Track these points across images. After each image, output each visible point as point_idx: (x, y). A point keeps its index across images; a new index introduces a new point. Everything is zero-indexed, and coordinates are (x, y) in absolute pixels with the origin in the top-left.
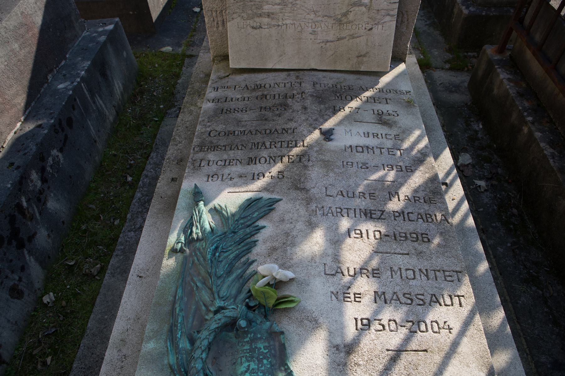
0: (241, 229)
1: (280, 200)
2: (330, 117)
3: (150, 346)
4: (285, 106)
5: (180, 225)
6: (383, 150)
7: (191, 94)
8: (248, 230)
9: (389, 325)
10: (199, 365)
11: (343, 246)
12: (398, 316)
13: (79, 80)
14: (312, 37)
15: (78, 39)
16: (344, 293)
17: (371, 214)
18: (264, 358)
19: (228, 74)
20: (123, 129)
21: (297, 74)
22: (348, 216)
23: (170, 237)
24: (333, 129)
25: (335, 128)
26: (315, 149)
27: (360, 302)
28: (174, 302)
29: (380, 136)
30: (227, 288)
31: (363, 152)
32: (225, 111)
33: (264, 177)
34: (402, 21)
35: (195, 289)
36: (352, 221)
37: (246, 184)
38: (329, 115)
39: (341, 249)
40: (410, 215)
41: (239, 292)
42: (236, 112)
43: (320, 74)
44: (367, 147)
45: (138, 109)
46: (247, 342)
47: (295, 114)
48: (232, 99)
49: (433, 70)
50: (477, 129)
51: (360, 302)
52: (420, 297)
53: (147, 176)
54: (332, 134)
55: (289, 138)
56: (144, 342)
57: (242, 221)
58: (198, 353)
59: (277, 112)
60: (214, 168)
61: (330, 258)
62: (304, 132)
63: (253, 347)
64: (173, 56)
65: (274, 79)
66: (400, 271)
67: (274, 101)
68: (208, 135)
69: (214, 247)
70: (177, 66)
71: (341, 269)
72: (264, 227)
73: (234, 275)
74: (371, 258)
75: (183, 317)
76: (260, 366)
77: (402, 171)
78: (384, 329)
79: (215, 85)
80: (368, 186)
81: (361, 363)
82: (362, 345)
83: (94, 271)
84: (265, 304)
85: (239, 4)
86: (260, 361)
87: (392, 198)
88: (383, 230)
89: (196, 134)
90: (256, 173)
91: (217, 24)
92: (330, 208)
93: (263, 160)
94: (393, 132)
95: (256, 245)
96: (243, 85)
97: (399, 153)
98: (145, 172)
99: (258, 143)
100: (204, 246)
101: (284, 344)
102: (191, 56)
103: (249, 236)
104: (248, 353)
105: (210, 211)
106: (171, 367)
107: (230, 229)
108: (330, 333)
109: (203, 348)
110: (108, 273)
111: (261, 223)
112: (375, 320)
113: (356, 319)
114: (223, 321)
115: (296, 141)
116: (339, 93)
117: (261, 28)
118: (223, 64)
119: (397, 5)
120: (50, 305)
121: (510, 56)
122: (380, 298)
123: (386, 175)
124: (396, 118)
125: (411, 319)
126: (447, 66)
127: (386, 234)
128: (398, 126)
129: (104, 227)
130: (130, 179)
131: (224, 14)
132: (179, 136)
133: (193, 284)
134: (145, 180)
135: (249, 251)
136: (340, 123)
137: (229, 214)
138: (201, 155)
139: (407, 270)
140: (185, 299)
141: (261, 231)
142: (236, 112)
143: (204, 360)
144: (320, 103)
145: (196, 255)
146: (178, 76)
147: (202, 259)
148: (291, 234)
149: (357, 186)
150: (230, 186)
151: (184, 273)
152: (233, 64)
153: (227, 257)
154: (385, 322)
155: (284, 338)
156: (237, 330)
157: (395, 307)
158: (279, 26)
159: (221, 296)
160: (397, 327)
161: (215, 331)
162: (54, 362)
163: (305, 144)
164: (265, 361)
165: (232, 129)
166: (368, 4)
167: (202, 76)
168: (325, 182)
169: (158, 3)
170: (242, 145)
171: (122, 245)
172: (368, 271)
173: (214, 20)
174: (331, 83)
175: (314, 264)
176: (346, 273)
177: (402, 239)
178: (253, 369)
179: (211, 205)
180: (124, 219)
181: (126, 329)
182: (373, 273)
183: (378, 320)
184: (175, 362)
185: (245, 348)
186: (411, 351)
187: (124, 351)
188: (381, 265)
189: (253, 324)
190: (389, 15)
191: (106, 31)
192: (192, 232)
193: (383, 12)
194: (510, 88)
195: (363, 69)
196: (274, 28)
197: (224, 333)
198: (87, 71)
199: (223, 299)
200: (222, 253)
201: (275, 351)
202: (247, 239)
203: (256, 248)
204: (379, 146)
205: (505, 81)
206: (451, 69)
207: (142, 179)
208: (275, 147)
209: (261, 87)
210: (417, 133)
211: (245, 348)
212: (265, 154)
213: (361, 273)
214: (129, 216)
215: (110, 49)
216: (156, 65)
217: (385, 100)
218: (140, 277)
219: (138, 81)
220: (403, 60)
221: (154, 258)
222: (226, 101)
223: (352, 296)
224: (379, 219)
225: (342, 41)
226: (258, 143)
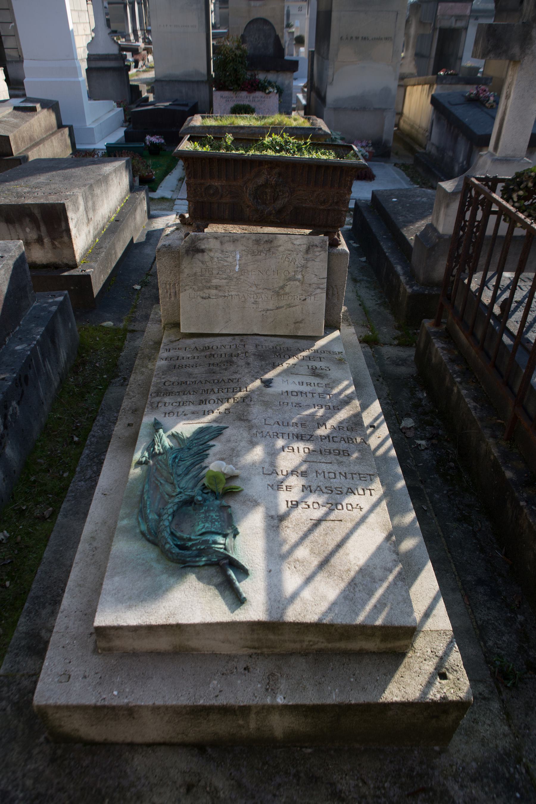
0: (195, 446)
1: (227, 427)
2: (270, 371)
3: (125, 522)
4: (231, 363)
5: (143, 447)
6: (314, 395)
7: (141, 358)
8: (201, 447)
10: (167, 523)
11: (278, 457)
12: (321, 501)
13: (35, 342)
14: (254, 306)
15: (30, 308)
16: (278, 486)
17: (302, 437)
19: (178, 338)
20: (67, 396)
21: (241, 338)
25: (276, 378)
26: (256, 393)
29: (312, 384)
30: (186, 482)
31: (297, 395)
32: (177, 366)
33: (213, 412)
34: (333, 294)
35: (159, 484)
37: (198, 418)
41: (195, 486)
43: (262, 339)
44: (301, 392)
45: (80, 378)
46: (203, 513)
47: (239, 368)
49: (381, 346)
50: (422, 397)
52: (338, 489)
53: (94, 436)
54: (271, 383)
55: (234, 385)
57: (196, 441)
59: (224, 367)
60: (170, 408)
64: (116, 331)
65: (221, 342)
67: (221, 359)
69: (174, 456)
70: (119, 340)
72: (214, 445)
73: (191, 475)
74: (300, 465)
77: (330, 409)
79: (167, 347)
80: (300, 418)
81: (290, 526)
82: (291, 516)
83: (47, 514)
84: (215, 490)
85: (190, 278)
86: (213, 523)
87: (320, 427)
89: (152, 384)
90: (207, 410)
91: (170, 295)
92: (268, 432)
93: (212, 402)
94: (324, 382)
96: (193, 347)
97: (328, 396)
98: (92, 433)
99: (208, 390)
102: (133, 331)
103: (201, 451)
105: (168, 437)
106: (143, 533)
108: (267, 508)
109: (169, 513)
111: (211, 443)
113: (287, 501)
114: (184, 497)
115: (240, 388)
117: (210, 298)
119: (326, 280)
120: (4, 542)
121: (446, 329)
123: (316, 412)
124: (328, 372)
126: (396, 342)
130: (76, 439)
131: (177, 287)
132: (133, 392)
135: (202, 460)
136: (279, 375)
137: (185, 437)
138: (158, 399)
139: (329, 473)
140: (152, 492)
144: (261, 360)
145: (159, 464)
146: (120, 349)
147: (164, 466)
149: (292, 418)
150: (184, 420)
151: (148, 477)
153: (184, 464)
157: (319, 494)
158: (225, 296)
162: (11, 587)
163: (248, 390)
164: (216, 523)
165: (184, 380)
166: (301, 279)
167: (151, 343)
168: (264, 415)
169: (99, 279)
170: (194, 391)
171: (73, 492)
172: (298, 473)
173: (167, 292)
174: (271, 345)
176: (280, 473)
178: (207, 527)
179: (169, 433)
180: (73, 472)
184: (146, 528)
187: (95, 544)
190: (319, 288)
191: (56, 302)
192: (154, 449)
193: (314, 286)
194: (443, 355)
195: (300, 333)
196: (221, 299)
197: (184, 508)
198: (42, 336)
200: (180, 462)
203: (208, 459)
205: (439, 350)
206: (399, 345)
207: (89, 438)
209: (209, 348)
210: (346, 383)
211: (201, 516)
212: (214, 397)
214: (78, 469)
215: (59, 319)
216: (98, 339)
219: (81, 353)
220: (337, 328)
222: (178, 359)
225: (281, 310)
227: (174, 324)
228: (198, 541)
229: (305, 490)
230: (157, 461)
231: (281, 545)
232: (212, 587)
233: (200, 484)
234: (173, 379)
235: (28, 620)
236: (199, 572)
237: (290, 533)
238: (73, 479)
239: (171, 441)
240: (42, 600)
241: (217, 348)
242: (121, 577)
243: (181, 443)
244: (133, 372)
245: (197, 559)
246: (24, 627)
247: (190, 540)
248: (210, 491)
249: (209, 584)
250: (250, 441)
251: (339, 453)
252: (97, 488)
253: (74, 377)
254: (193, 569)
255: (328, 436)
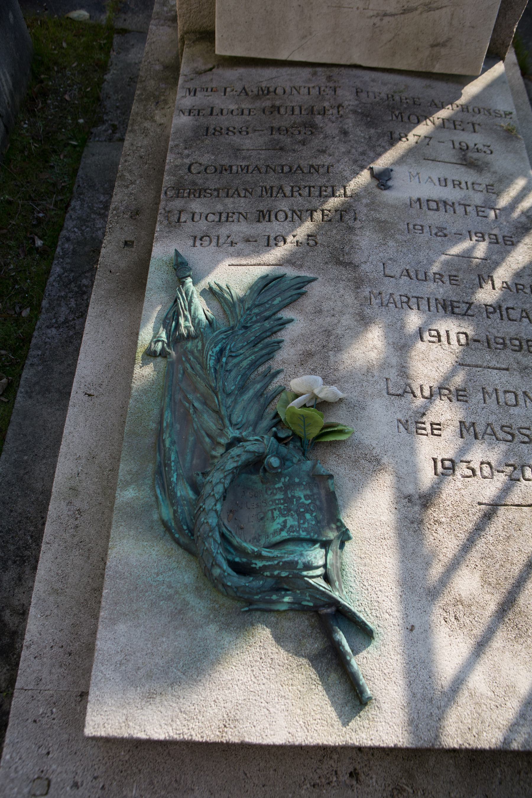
0: (256, 322)
1: (314, 280)
2: (386, 150)
5: (155, 314)
6: (469, 209)
8: (267, 324)
9: (481, 469)
10: (213, 520)
11: (413, 353)
12: (493, 457)
16: (417, 422)
17: (453, 307)
18: (307, 511)
19: (210, 66)
20: (19, 159)
21: (328, 73)
22: (419, 309)
23: (141, 333)
24: (392, 170)
26: (364, 201)
27: (440, 435)
28: (160, 432)
29: (463, 185)
30: (242, 410)
31: (437, 209)
32: (211, 131)
33: (285, 242)
35: (191, 411)
36: (425, 315)
37: (257, 252)
38: (383, 147)
39: (410, 357)
40: (510, 311)
41: (260, 417)
42: (230, 133)
43: (367, 76)
44: (445, 203)
45: (40, 124)
46: (280, 489)
47: (328, 142)
48: (222, 110)
51: (440, 435)
52: (524, 431)
53: (68, 239)
54: (390, 179)
55: (322, 181)
56: (119, 489)
57: (256, 311)
58: (209, 504)
59: (300, 138)
60: (202, 226)
61: (394, 370)
62: (345, 173)
63: (290, 496)
65: (290, 80)
66: (497, 393)
67: (293, 118)
68: (187, 171)
69: (218, 349)
70: (101, 48)
71: (411, 388)
72: (291, 321)
73: (251, 393)
74: (453, 372)
75: (177, 452)
76: (302, 522)
77: (497, 243)
78: (474, 474)
79: (191, 85)
80: (447, 263)
81: (443, 520)
82: (444, 496)
84: (302, 435)
86: (301, 516)
87: (484, 285)
88: (470, 332)
89: (167, 167)
90: (273, 235)
92: (391, 294)
93: (281, 216)
94: (485, 179)
95: (280, 348)
96: (238, 87)
98: (64, 233)
99: (272, 188)
100: (200, 347)
101: (333, 493)
102: (123, 32)
103: (268, 334)
104: (282, 504)
105: (203, 293)
106: (164, 523)
107: (239, 321)
108: (399, 478)
109: (217, 496)
110: (21, 393)
111: (286, 314)
112: (462, 461)
113: (435, 460)
114: (244, 458)
115: (333, 187)
116: (398, 109)
118: (199, 47)
122: (468, 431)
123: (474, 247)
125: (512, 462)
127: (476, 338)
128: (492, 170)
129: (5, 320)
130: (39, 243)
132: (130, 172)
133: (187, 405)
134: (66, 246)
136: (401, 160)
137: (235, 299)
138: (178, 203)
139: (506, 392)
140: (178, 426)
141: (287, 326)
142: (230, 133)
143: (219, 513)
144: (371, 124)
145: (188, 360)
146: (104, 67)
147: (198, 367)
148: (334, 332)
149: (431, 262)
150: (232, 256)
152: (222, 48)
153: (237, 365)
154: (476, 465)
155: (332, 484)
156: (265, 470)
157: (490, 444)
159: (234, 422)
160: (492, 473)
161: (233, 472)
163: (349, 193)
164: (308, 516)
165: (226, 162)
168: (381, 254)
170: (246, 190)
171: (39, 349)
172: (450, 391)
174: (385, 90)
175: (371, 379)
176: (418, 393)
177: (499, 346)
178: (292, 526)
179: (204, 284)
180: (37, 308)
181: (75, 471)
182: (458, 395)
183: (466, 462)
184: (171, 516)
185: (277, 497)
186: (512, 505)
187: (78, 504)
188: (469, 384)
189: (288, 463)
192: (178, 324)
195: (438, 69)
197: (243, 476)
199: (238, 427)
200: (230, 359)
201: (321, 501)
202: (266, 338)
203: (281, 352)
204: (462, 202)
207: (60, 243)
208: (300, 195)
209: (269, 92)
211: (277, 497)
212: (284, 205)
213: (440, 394)
214: (45, 303)
216: (64, 45)
217: (470, 125)
218: (89, 395)
220: (501, 58)
221: (108, 366)
222: (211, 114)
223: (429, 427)
224: (465, 315)
225: (410, 15)
226: (272, 188)
227: (201, 33)
228: (276, 562)
230: (185, 354)
231: (428, 565)
232: (304, 661)
233: (270, 412)
234: (206, 159)
236: (277, 623)
237: (444, 539)
238: (38, 323)
239: (208, 304)
241: (284, 92)
242: (130, 623)
243: (228, 312)
244: (129, 128)
245: (274, 597)
247: (259, 556)
248: (290, 433)
249: (297, 654)
250: (359, 314)
252: (75, 380)
253: (29, 120)
254: (266, 614)
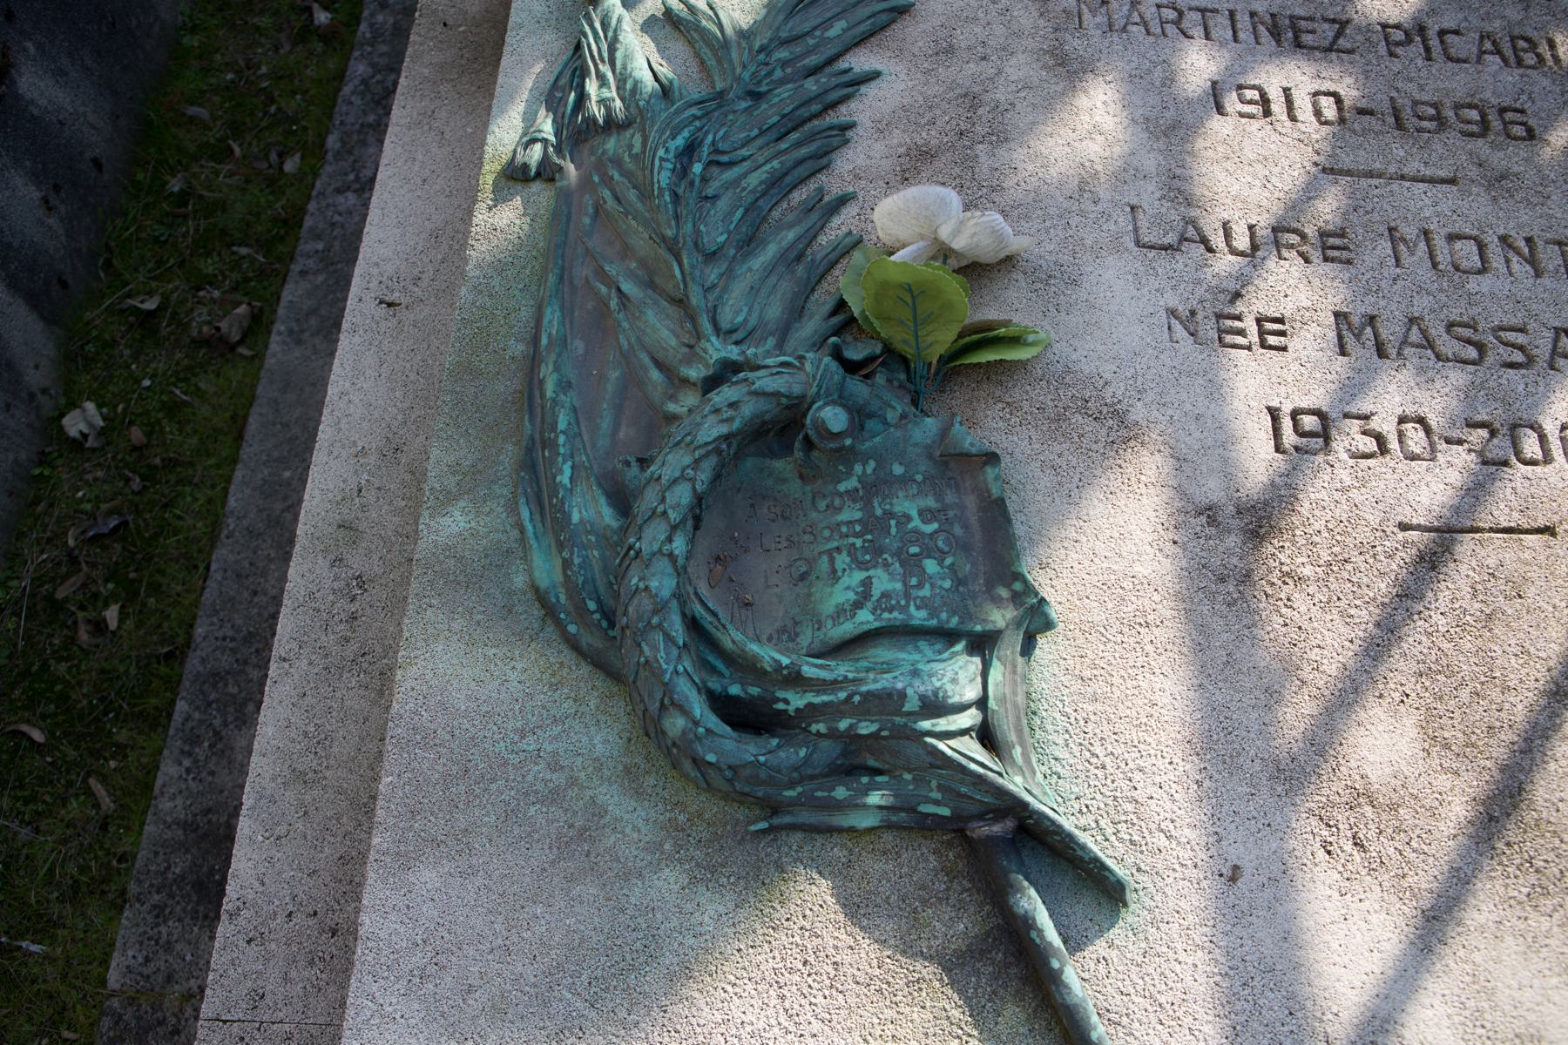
3: (452, 525)
5: (529, 83)
8: (811, 86)
9: (1401, 436)
10: (662, 582)
11: (1200, 144)
16: (1220, 316)
17: (1297, 33)
18: (927, 552)
22: (1207, 37)
23: (493, 128)
27: (1284, 349)
28: (533, 361)
30: (747, 294)
35: (613, 304)
36: (1225, 52)
39: (1192, 153)
40: (1449, 38)
41: (797, 311)
46: (852, 494)
51: (1284, 349)
52: (1511, 336)
56: (426, 514)
57: (783, 54)
58: (652, 537)
61: (1151, 187)
63: (879, 512)
66: (1428, 241)
69: (680, 141)
71: (1198, 229)
72: (874, 75)
73: (771, 251)
74: (1310, 192)
75: (574, 410)
76: (914, 581)
78: (1383, 449)
81: (1307, 571)
82: (1304, 508)
83: (231, 327)
84: (909, 351)
86: (911, 565)
88: (1349, 90)
95: (847, 142)
100: (637, 149)
101: (1000, 503)
103: (815, 108)
104: (856, 535)
105: (649, 26)
106: (541, 597)
107: (739, 79)
108: (1180, 460)
109: (673, 516)
110: (280, 334)
111: (860, 61)
112: (1346, 416)
113: (1274, 413)
114: (748, 410)
120: (90, 443)
122: (1358, 336)
125: (1483, 416)
127: (1363, 104)
129: (247, 181)
130: (322, 17)
133: (603, 289)
134: (380, 18)
135: (821, 160)
137: (729, 30)
139: (1452, 238)
140: (579, 346)
141: (863, 89)
143: (681, 561)
145: (607, 181)
147: (632, 195)
148: (986, 97)
151: (559, 253)
153: (736, 182)
154: (1388, 427)
155: (997, 478)
156: (809, 444)
157: (1421, 370)
159: (725, 324)
160: (1432, 445)
161: (718, 451)
162: (129, 624)
164: (931, 566)
171: (319, 237)
172: (1303, 236)
175: (1091, 207)
176: (1218, 241)
177: (1426, 124)
178: (885, 595)
181: (353, 483)
182: (1325, 248)
183: (1358, 417)
184: (559, 578)
185: (844, 516)
186: (1491, 530)
187: (357, 562)
188: (1353, 217)
189: (871, 424)
192: (582, 97)
197: (750, 463)
199: (736, 337)
200: (715, 170)
201: (965, 526)
202: (810, 119)
203: (848, 152)
207: (366, 13)
211: (844, 516)
213: (1277, 244)
214: (332, 141)
218: (390, 305)
221: (435, 236)
223: (1253, 329)
224: (1329, 49)
228: (842, 695)
229: (1349, 339)
230: (600, 166)
231: (1272, 696)
232: (928, 970)
233: (822, 301)
235: (188, 771)
236: (849, 864)
238: (318, 184)
239: (661, 50)
240: (233, 689)
242: (447, 866)
243: (712, 62)
245: (840, 793)
246: (179, 801)
247: (795, 679)
248: (878, 349)
249: (907, 949)
250: (1051, 52)
251: (1484, 124)
252: (358, 270)
254: (820, 840)
255: (1419, 29)
